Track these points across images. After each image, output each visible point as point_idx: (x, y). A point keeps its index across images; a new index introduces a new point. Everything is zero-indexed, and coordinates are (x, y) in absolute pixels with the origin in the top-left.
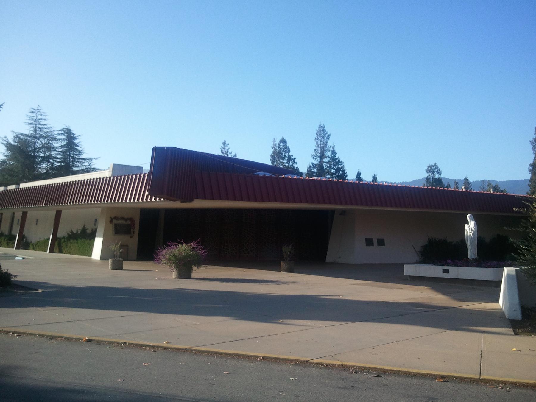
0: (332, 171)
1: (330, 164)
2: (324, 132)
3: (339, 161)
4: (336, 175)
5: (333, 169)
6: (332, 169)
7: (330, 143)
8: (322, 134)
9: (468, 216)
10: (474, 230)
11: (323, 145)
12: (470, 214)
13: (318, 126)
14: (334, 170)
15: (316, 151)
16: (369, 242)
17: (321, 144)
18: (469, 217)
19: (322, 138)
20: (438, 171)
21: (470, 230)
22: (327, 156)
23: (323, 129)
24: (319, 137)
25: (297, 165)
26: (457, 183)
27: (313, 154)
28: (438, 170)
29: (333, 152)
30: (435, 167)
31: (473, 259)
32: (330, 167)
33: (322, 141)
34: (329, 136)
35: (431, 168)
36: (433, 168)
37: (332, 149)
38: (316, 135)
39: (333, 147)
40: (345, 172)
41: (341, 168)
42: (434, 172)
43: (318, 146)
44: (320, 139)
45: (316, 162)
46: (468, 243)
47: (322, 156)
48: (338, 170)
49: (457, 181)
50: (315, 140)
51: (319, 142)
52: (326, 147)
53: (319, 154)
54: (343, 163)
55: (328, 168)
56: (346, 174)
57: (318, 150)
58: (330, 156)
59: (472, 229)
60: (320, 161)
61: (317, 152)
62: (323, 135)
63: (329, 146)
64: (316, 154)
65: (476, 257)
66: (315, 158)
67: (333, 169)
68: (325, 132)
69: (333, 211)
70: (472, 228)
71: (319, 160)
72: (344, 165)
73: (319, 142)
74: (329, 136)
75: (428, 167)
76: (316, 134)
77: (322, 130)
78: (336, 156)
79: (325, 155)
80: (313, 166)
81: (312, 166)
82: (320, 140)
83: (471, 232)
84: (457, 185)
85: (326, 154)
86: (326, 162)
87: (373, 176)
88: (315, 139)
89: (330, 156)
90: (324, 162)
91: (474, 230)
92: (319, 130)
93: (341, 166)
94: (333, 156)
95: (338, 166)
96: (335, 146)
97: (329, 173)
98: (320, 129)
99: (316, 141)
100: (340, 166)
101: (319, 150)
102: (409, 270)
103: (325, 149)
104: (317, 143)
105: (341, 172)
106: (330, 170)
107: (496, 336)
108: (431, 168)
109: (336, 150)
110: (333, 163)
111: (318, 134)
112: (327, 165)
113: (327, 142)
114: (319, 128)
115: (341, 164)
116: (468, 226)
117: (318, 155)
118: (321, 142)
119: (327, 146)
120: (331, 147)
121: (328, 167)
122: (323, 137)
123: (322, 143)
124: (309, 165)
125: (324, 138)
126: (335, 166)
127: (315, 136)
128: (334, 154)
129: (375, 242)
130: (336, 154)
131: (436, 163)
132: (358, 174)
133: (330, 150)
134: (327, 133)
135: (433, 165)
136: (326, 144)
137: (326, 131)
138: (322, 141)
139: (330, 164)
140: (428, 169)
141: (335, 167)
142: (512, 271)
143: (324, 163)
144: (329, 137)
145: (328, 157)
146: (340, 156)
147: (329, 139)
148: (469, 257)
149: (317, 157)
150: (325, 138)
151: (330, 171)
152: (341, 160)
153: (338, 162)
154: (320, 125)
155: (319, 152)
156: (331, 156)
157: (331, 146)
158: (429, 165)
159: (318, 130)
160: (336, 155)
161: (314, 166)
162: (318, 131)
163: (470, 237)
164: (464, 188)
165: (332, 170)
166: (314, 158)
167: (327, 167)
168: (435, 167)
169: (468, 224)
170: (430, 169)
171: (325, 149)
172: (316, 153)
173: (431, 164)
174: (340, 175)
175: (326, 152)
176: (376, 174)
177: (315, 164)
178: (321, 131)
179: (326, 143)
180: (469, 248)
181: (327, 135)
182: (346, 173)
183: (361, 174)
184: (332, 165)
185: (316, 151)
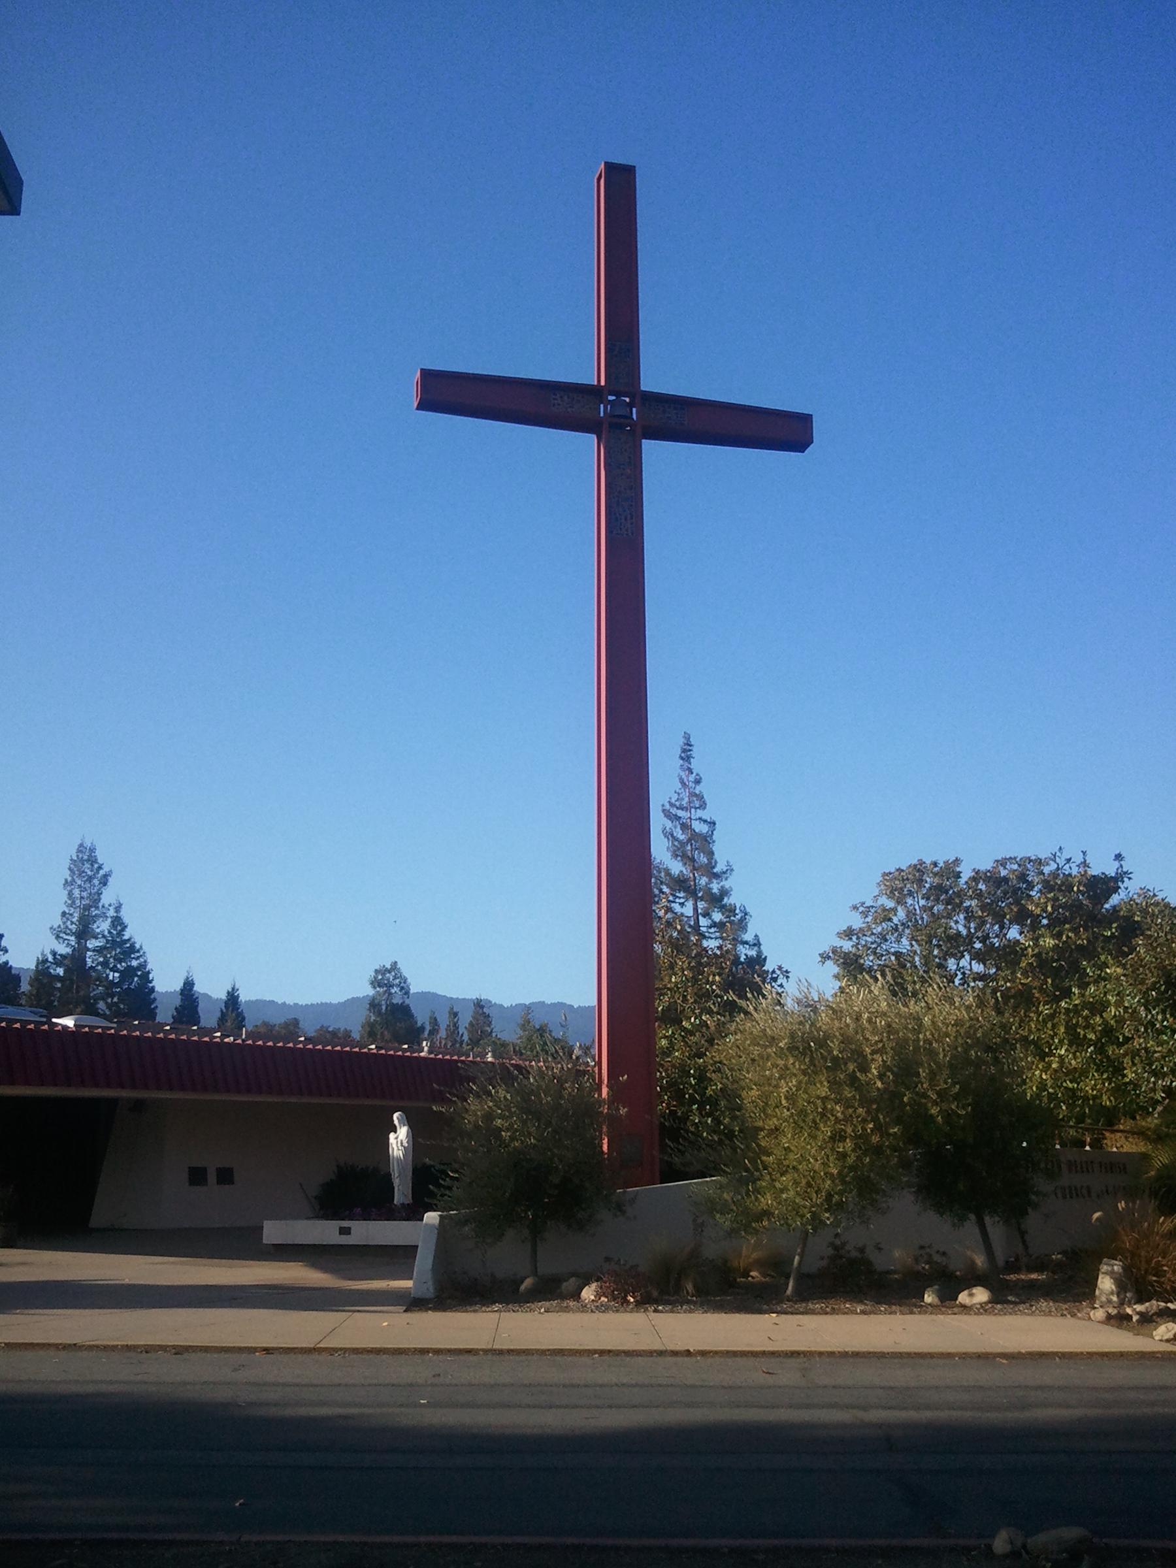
0: (111, 978)
1: (105, 957)
2: (92, 865)
3: (132, 949)
4: (122, 988)
5: (114, 970)
6: (111, 970)
7: (107, 898)
8: (86, 870)
9: (396, 1116)
10: (406, 1145)
11: (87, 902)
12: (399, 1113)
13: (77, 847)
14: (117, 975)
15: (67, 916)
16: (197, 1176)
17: (82, 898)
18: (398, 1118)
19: (87, 880)
20: (400, 983)
21: (399, 1145)
22: (98, 934)
23: (90, 856)
24: (77, 880)
25: (7, 955)
26: (456, 1015)
27: (55, 926)
28: (402, 981)
29: (117, 922)
30: (393, 973)
31: (403, 1204)
32: (105, 964)
33: (86, 890)
34: (106, 876)
35: (384, 974)
36: (388, 975)
37: (115, 914)
38: (69, 872)
39: (116, 908)
40: (149, 978)
41: (137, 967)
42: (392, 986)
43: (74, 902)
44: (79, 882)
45: (63, 949)
46: (395, 1174)
47: (84, 933)
48: (128, 973)
49: (455, 1010)
50: (64, 885)
51: (76, 892)
52: (97, 908)
53: (74, 926)
54: (144, 953)
55: (100, 967)
56: (151, 985)
57: (71, 915)
58: (106, 933)
59: (402, 1143)
60: (76, 946)
61: (68, 919)
62: (89, 873)
63: (106, 906)
64: (67, 927)
65: (409, 1201)
66: (62, 938)
67: (114, 972)
68: (96, 866)
69: (113, 1102)
70: (402, 1141)
71: (73, 943)
72: (145, 961)
73: (76, 892)
74: (106, 876)
75: (377, 971)
76: (70, 869)
77: (86, 857)
78: (124, 933)
79: (93, 930)
80: (55, 958)
81: (50, 958)
82: (80, 886)
83: (400, 1148)
84: (456, 1020)
85: (95, 926)
86: (94, 951)
87: (228, 993)
88: (63, 882)
89: (106, 933)
90: (88, 950)
91: (406, 1145)
92: (78, 856)
93: (138, 961)
94: (115, 932)
95: (129, 964)
96: (123, 906)
97: (101, 982)
98: (80, 856)
99: (69, 888)
100: (135, 963)
101: (76, 915)
102: (273, 1232)
103: (94, 914)
104: (69, 894)
105: (136, 979)
106: (105, 972)
107: (372, 1314)
108: (384, 974)
109: (125, 915)
110: (115, 954)
111: (75, 869)
112: (97, 959)
113: (99, 894)
114: (79, 851)
115: (138, 958)
116: (396, 1135)
117: (70, 929)
118: (81, 891)
119: (100, 905)
120: (111, 908)
121: (98, 964)
122: (90, 879)
123: (85, 894)
124: (42, 954)
125: (90, 882)
126: (120, 961)
127: (67, 875)
128: (119, 928)
129: (212, 1177)
130: (126, 927)
131: (396, 963)
132: (185, 984)
133: (107, 917)
134: (100, 868)
135: (389, 967)
136: (95, 900)
137: (100, 861)
138: (86, 890)
139: (105, 957)
140: (374, 977)
141: (119, 966)
142: (434, 1218)
143: (89, 953)
144: (107, 880)
145: (100, 936)
146: (134, 932)
147: (105, 884)
148: (395, 1202)
149: (67, 934)
150: (96, 882)
151: (104, 975)
152: (137, 946)
153: (130, 950)
154: (81, 845)
155: (74, 920)
156: (110, 932)
157: (110, 905)
158: (378, 967)
159: (76, 858)
160: (123, 929)
161: (59, 960)
162: (75, 861)
163: (398, 1159)
164: (427, 1045)
165: (112, 973)
166: (58, 937)
167: (97, 966)
168: (393, 973)
169: (396, 1132)
170: (380, 977)
171: (94, 912)
172: (64, 923)
173: (384, 966)
174: (132, 987)
175: (95, 922)
176: (237, 987)
177: (61, 955)
178: (82, 861)
179: (96, 897)
180: (396, 1182)
181: (102, 872)
182: (151, 982)
183: (194, 984)
184: (112, 960)
185: (67, 916)
